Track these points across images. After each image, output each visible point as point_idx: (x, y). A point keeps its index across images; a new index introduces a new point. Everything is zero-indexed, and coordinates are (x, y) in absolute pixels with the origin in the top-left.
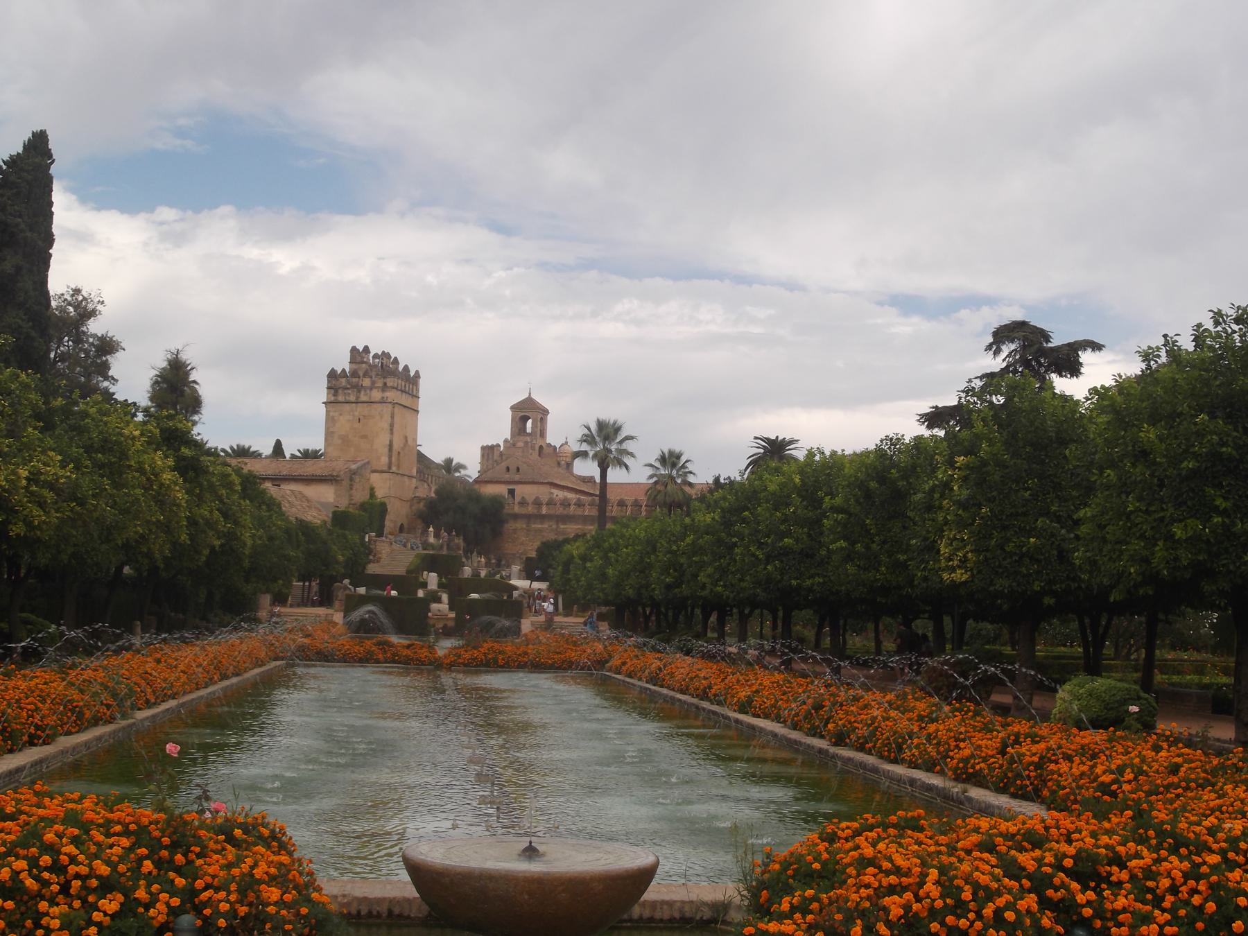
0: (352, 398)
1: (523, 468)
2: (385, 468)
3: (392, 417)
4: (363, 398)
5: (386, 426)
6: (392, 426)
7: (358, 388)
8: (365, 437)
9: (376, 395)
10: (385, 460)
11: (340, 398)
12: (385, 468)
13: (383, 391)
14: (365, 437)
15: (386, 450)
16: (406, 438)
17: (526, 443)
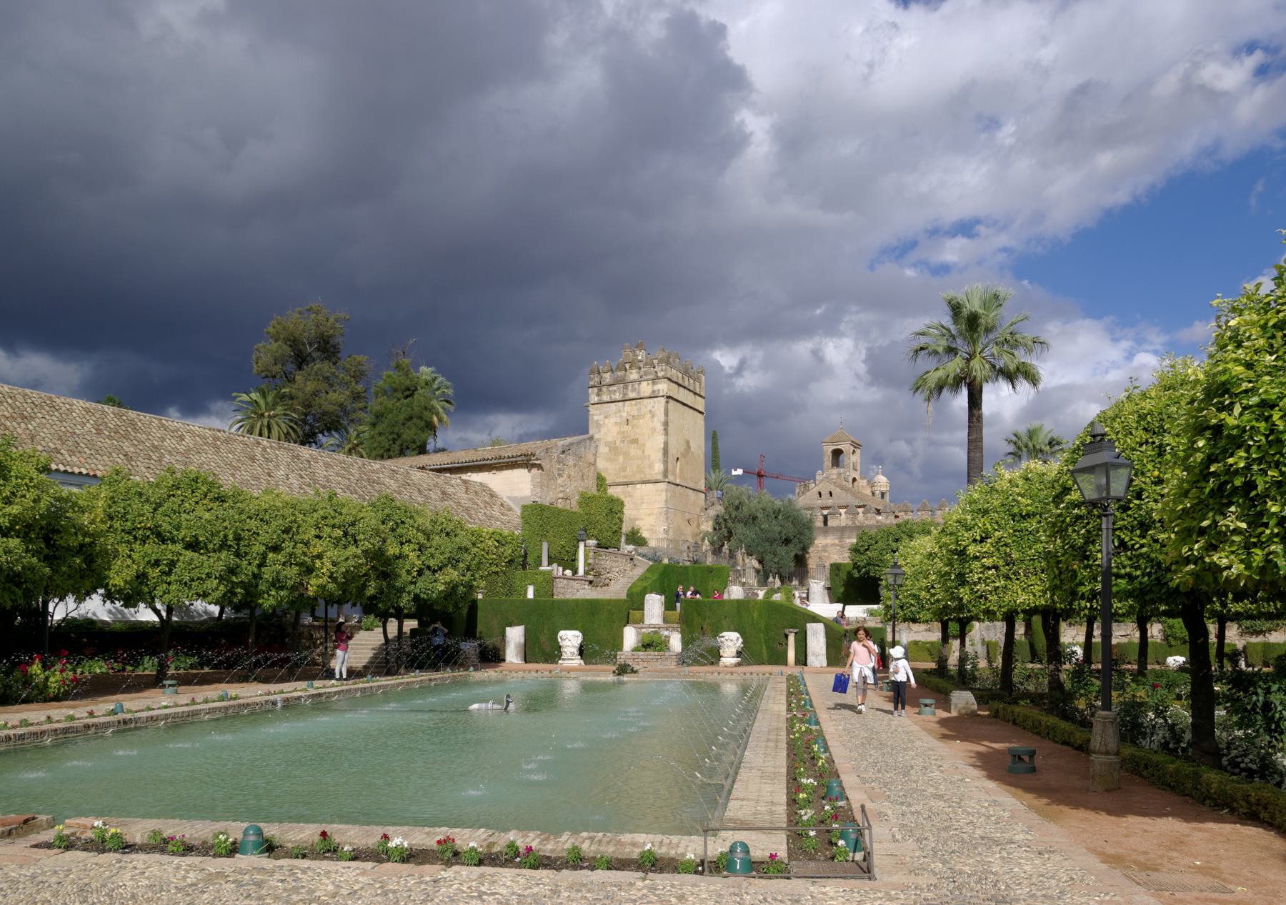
0: (618, 396)
1: (836, 491)
2: (660, 477)
3: (666, 414)
4: (632, 395)
5: (660, 427)
6: (666, 424)
7: (622, 382)
8: (635, 441)
9: (646, 388)
10: (659, 467)
11: (605, 398)
12: (660, 477)
13: (654, 383)
14: (635, 441)
15: (660, 455)
16: (688, 443)
17: (839, 474)
